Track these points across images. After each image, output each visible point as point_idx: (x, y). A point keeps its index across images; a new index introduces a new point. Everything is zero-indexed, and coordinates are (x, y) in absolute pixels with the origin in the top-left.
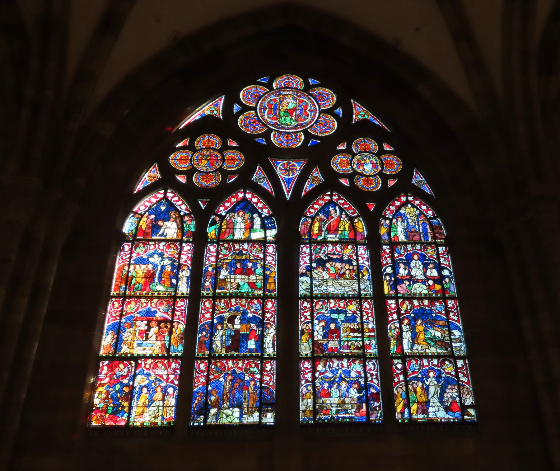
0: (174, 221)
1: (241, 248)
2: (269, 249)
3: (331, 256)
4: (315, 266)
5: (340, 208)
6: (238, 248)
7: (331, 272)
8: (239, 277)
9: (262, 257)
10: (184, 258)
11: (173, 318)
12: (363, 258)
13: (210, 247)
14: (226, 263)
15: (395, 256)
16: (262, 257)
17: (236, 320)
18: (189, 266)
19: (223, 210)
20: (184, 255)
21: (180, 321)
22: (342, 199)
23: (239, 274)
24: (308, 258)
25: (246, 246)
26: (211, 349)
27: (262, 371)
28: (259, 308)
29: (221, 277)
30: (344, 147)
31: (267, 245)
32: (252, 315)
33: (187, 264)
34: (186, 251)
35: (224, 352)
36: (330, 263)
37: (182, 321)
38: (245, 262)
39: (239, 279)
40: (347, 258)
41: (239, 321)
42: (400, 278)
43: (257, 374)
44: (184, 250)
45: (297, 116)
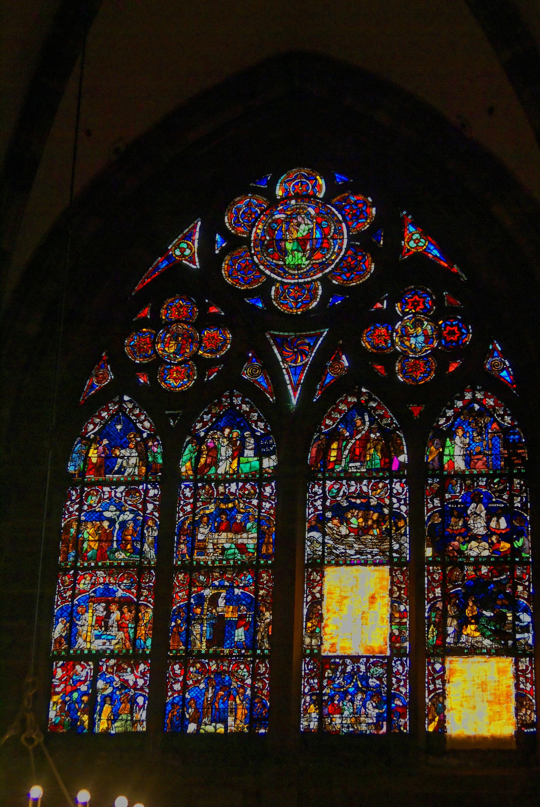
0: (133, 448)
1: (227, 490)
2: (265, 491)
3: (353, 500)
4: (330, 517)
5: (370, 416)
6: (223, 491)
7: (352, 526)
8: (224, 535)
9: (256, 504)
10: (150, 507)
11: (139, 600)
12: (399, 500)
13: (185, 490)
14: (207, 515)
15: (447, 497)
16: (256, 504)
17: (220, 600)
18: (157, 520)
19: (201, 428)
20: (150, 503)
21: (148, 604)
22: (375, 400)
23: (224, 531)
24: (319, 503)
25: (233, 487)
26: (187, 643)
27: (255, 675)
28: (251, 581)
29: (200, 537)
30: (383, 304)
31: (264, 483)
32: (241, 592)
33: (154, 517)
34: (151, 497)
35: (204, 647)
36: (351, 511)
37: (150, 602)
38: (233, 513)
39: (223, 538)
40: (376, 503)
41: (225, 601)
42: (451, 532)
43: (247, 679)
44: (150, 495)
45: (313, 250)
